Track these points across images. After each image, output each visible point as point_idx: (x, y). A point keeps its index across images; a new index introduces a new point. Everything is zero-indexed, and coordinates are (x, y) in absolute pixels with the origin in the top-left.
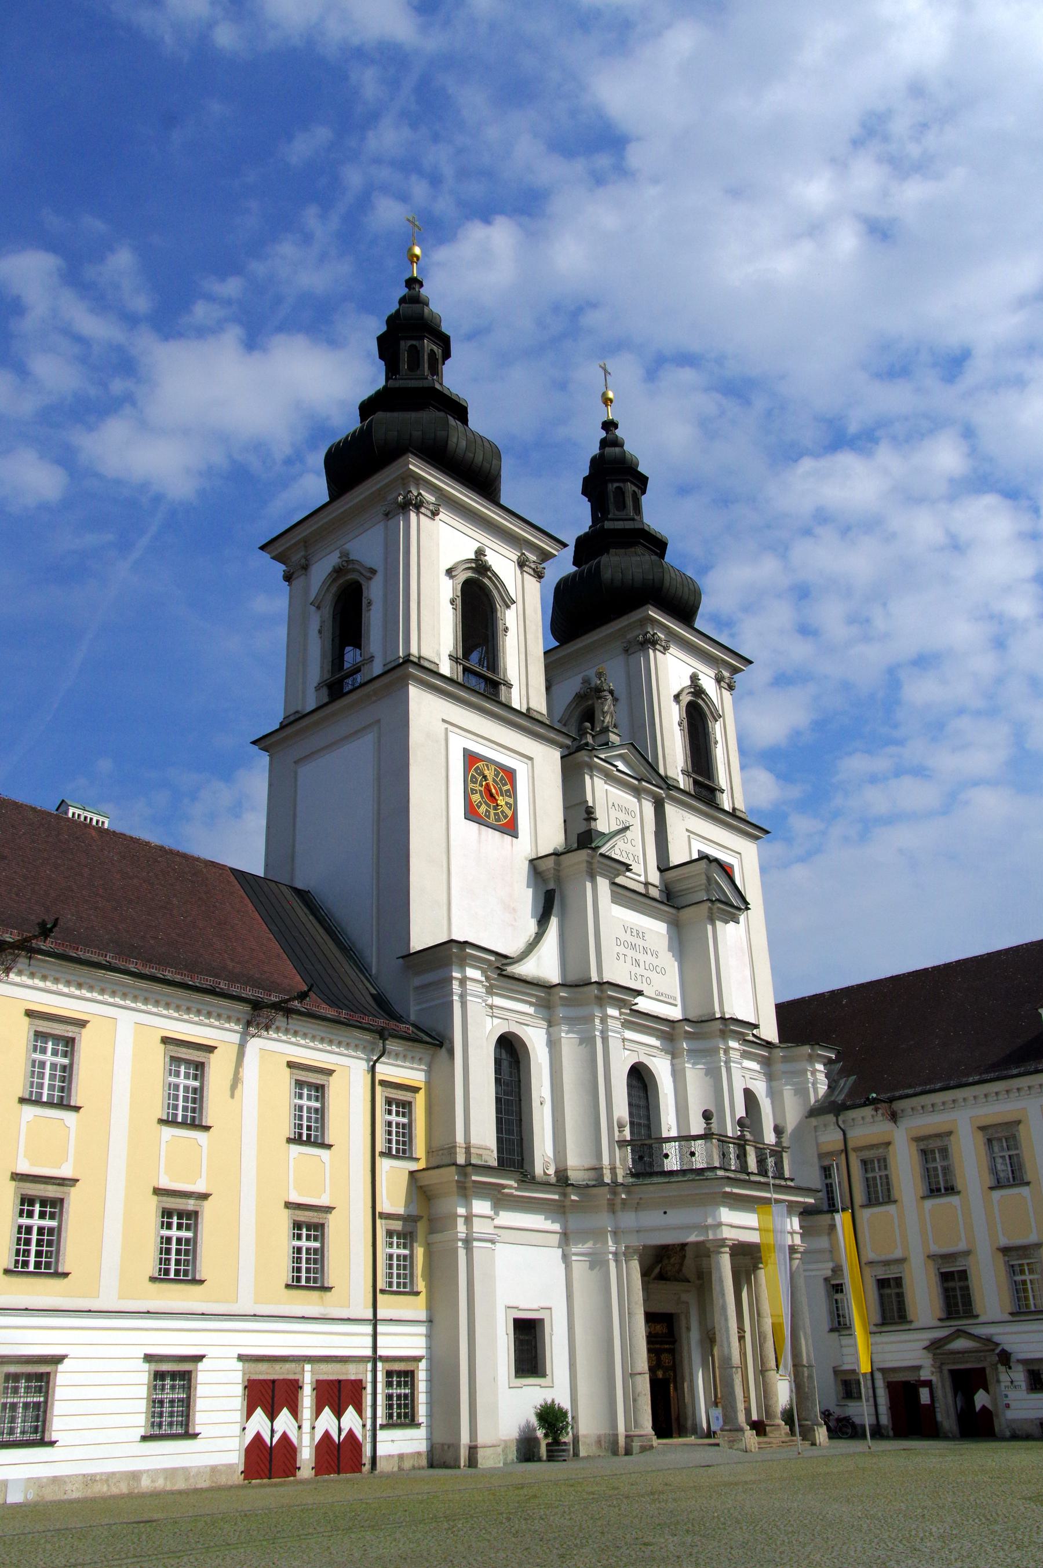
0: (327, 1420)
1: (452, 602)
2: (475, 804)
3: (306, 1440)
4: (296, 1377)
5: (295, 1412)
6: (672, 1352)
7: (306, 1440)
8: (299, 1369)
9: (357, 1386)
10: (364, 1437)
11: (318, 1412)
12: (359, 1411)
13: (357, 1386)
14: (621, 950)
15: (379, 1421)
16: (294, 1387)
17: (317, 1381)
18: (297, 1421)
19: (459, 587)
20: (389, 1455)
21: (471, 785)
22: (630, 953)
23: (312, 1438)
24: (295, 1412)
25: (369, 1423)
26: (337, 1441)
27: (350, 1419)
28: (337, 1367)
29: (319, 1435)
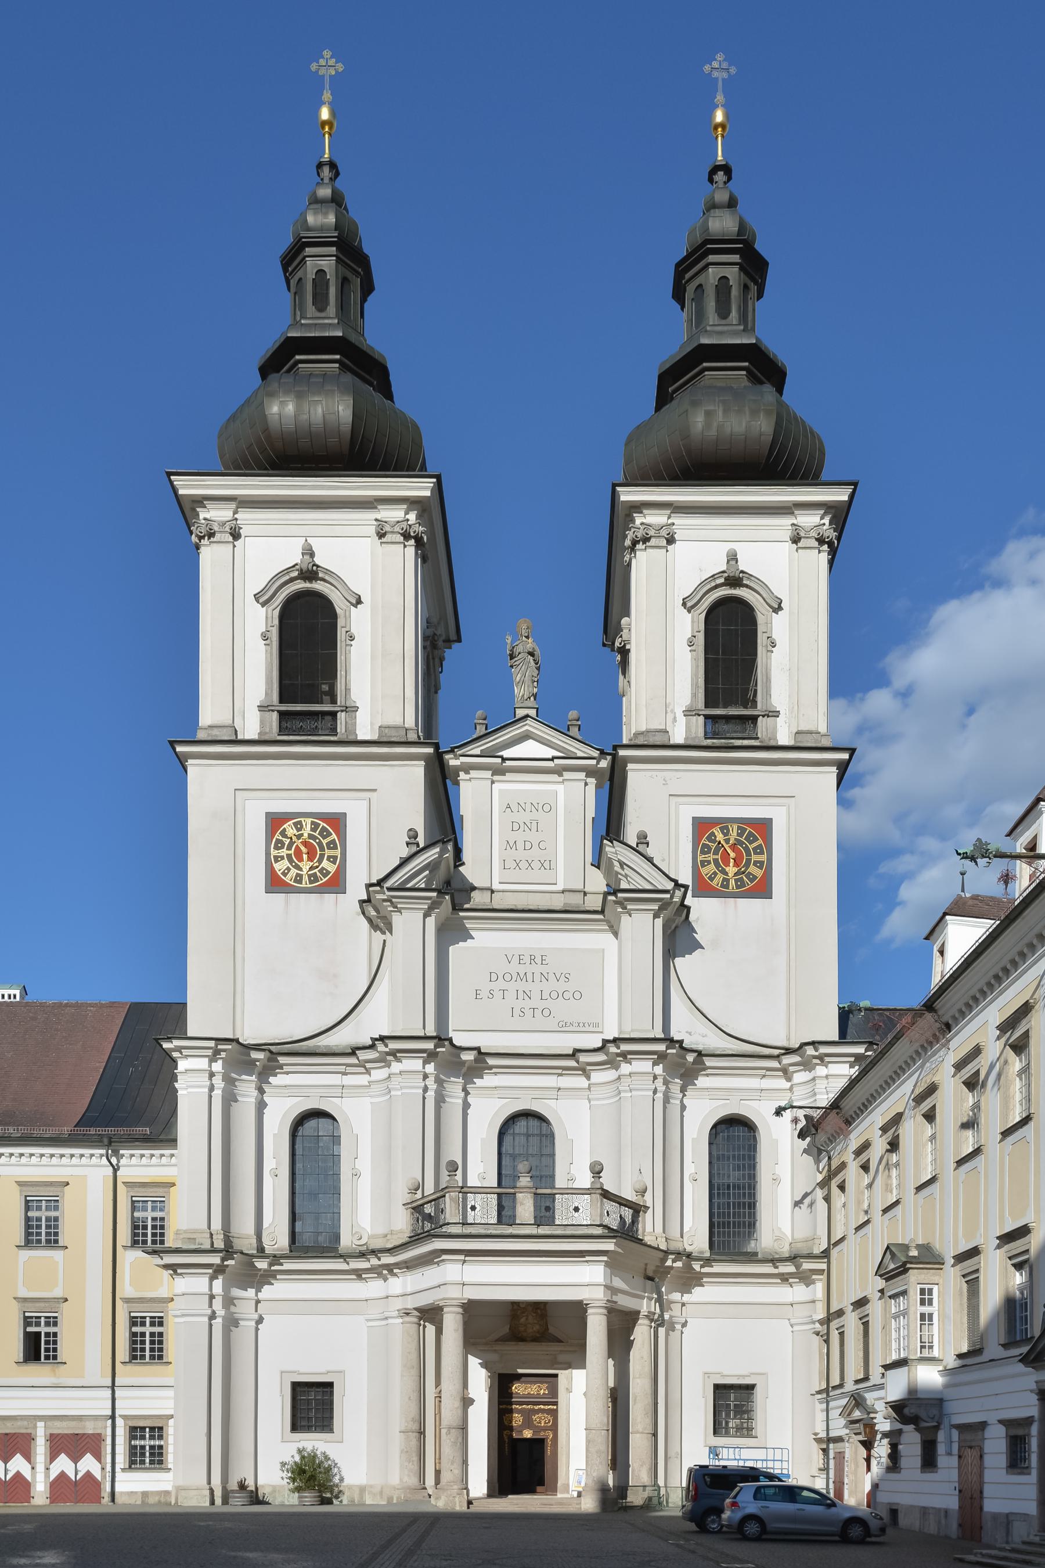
0: (63, 1464)
1: (265, 637)
2: (279, 873)
3: (40, 1477)
4: (29, 1431)
5: (28, 1457)
6: (554, 1413)
7: (40, 1477)
8: (31, 1425)
9: (98, 1438)
10: (104, 1477)
11: (53, 1457)
12: (98, 1457)
13: (98, 1438)
14: (501, 984)
15: (119, 1466)
16: (29, 1438)
17: (51, 1435)
18: (30, 1464)
19: (277, 612)
20: (132, 1492)
21: (274, 852)
22: (512, 987)
23: (47, 1476)
24: (28, 1457)
25: (109, 1468)
26: (74, 1480)
27: (88, 1464)
28: (73, 1424)
29: (54, 1474)
